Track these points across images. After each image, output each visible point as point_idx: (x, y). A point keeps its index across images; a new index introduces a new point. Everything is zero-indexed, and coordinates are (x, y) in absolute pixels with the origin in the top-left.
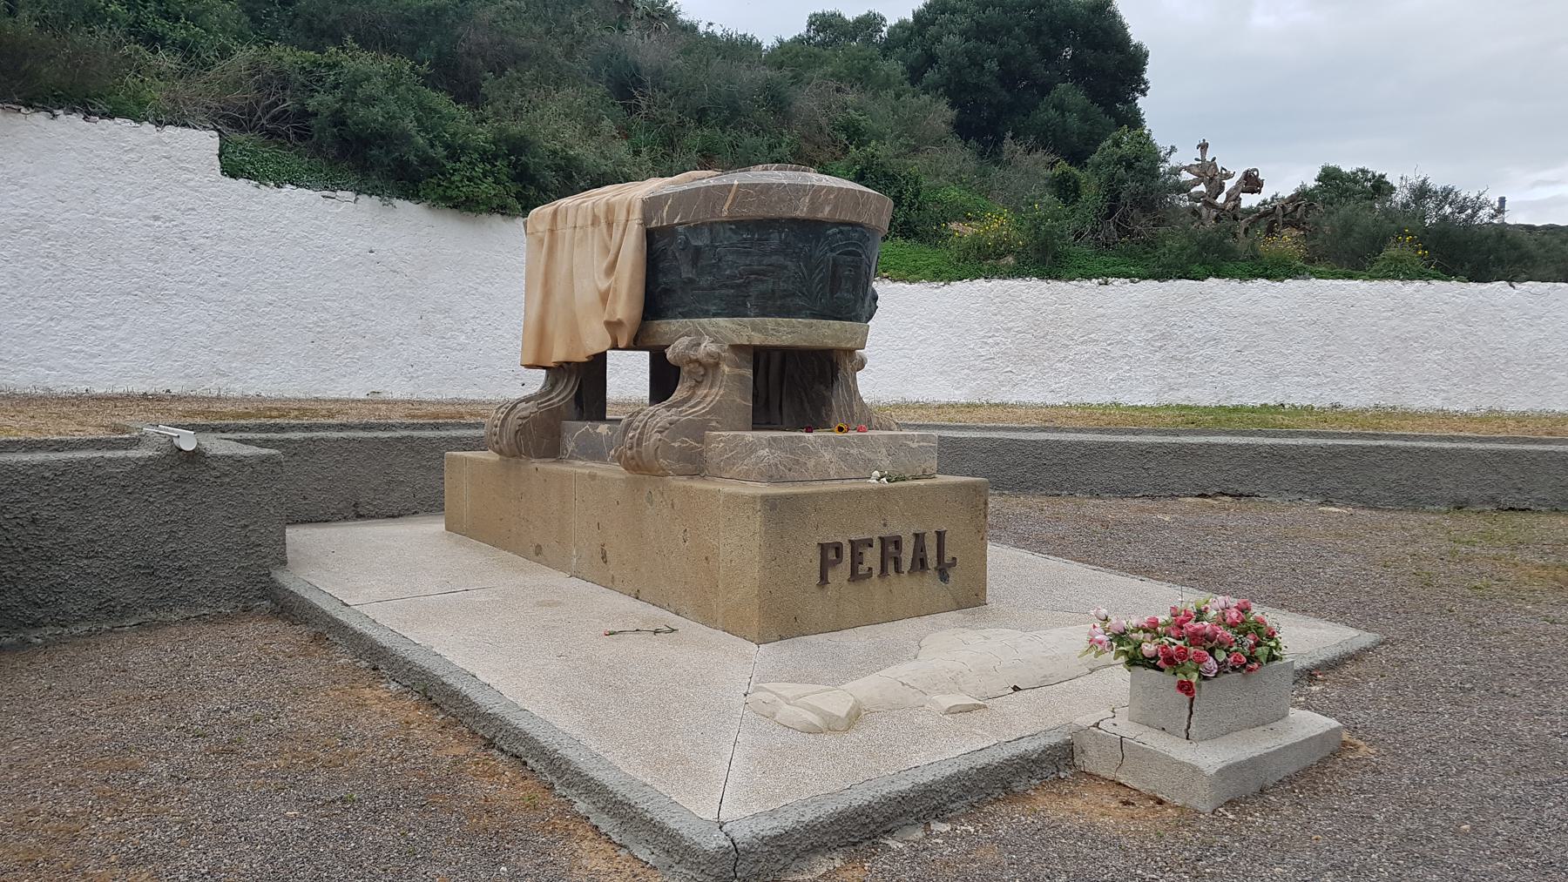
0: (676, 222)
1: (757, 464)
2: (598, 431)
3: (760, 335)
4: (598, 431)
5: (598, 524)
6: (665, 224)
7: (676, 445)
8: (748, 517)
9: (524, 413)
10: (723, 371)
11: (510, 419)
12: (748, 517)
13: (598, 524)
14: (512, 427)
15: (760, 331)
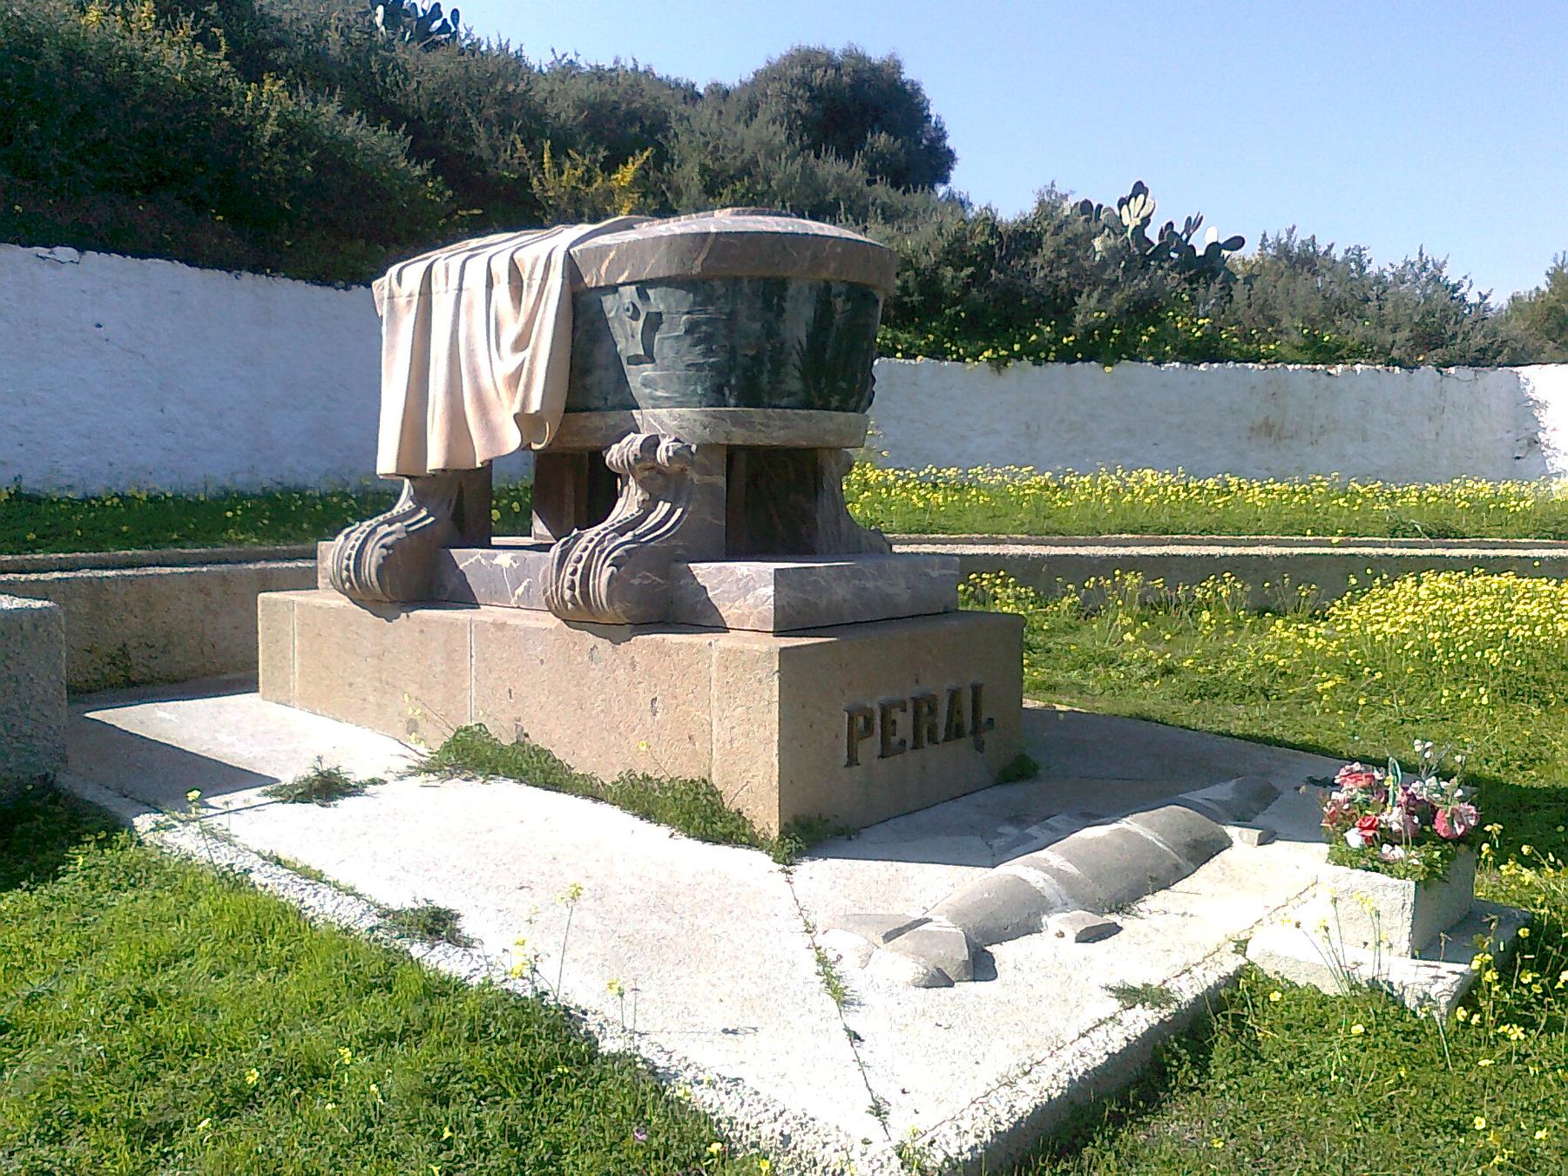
0: (620, 280)
1: (756, 607)
2: (495, 562)
3: (743, 431)
4: (495, 562)
5: (510, 691)
6: (602, 284)
7: (636, 582)
8: (760, 681)
9: (388, 540)
10: (692, 480)
11: (368, 548)
12: (760, 681)
13: (510, 691)
14: (374, 559)
15: (743, 425)
